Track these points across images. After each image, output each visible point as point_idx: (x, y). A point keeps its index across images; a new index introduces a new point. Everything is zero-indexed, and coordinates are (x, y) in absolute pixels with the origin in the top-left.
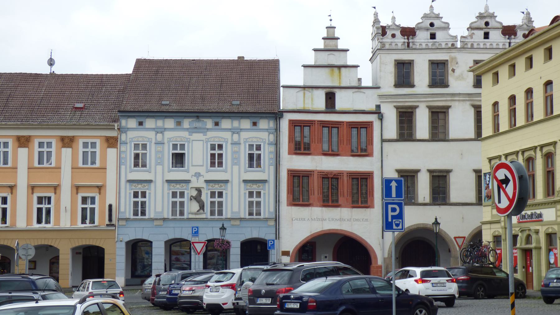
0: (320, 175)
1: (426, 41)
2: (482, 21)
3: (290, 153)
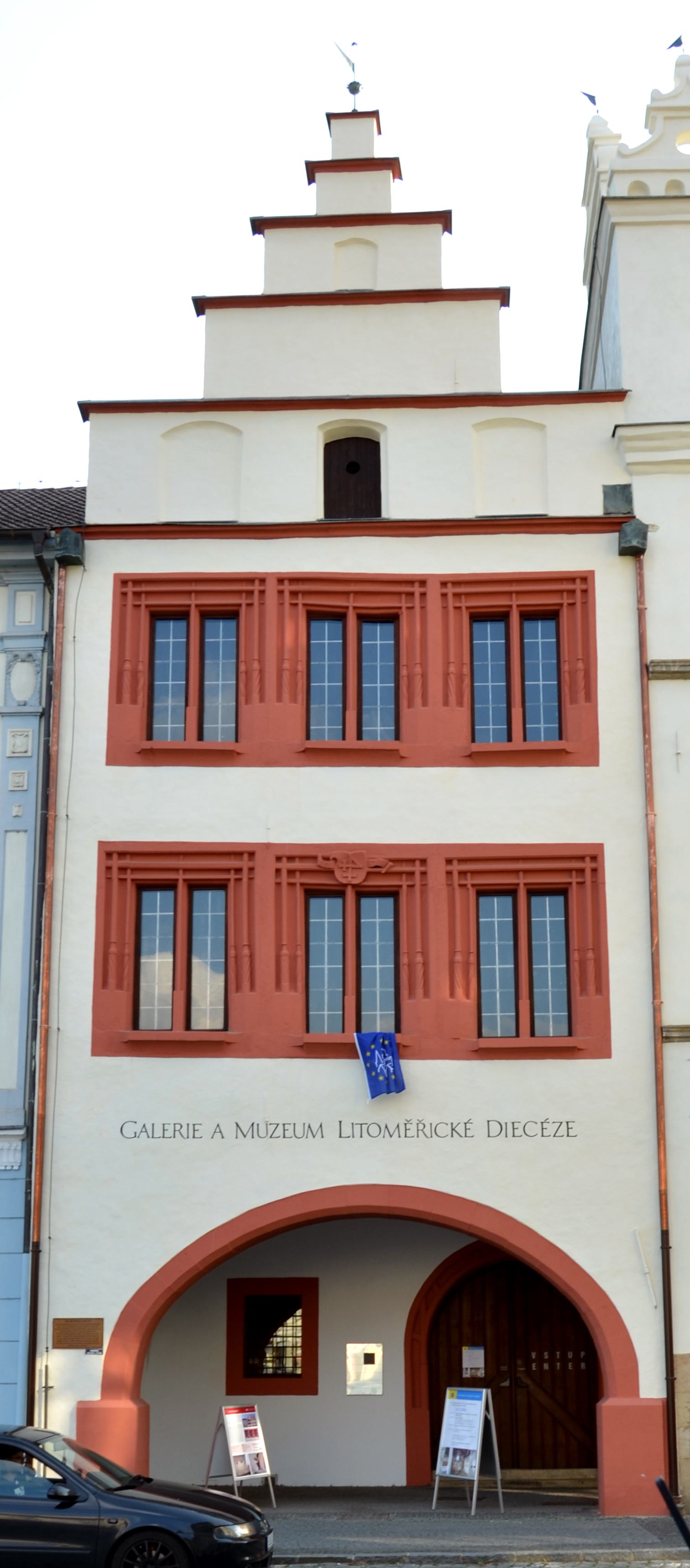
0: (291, 872)
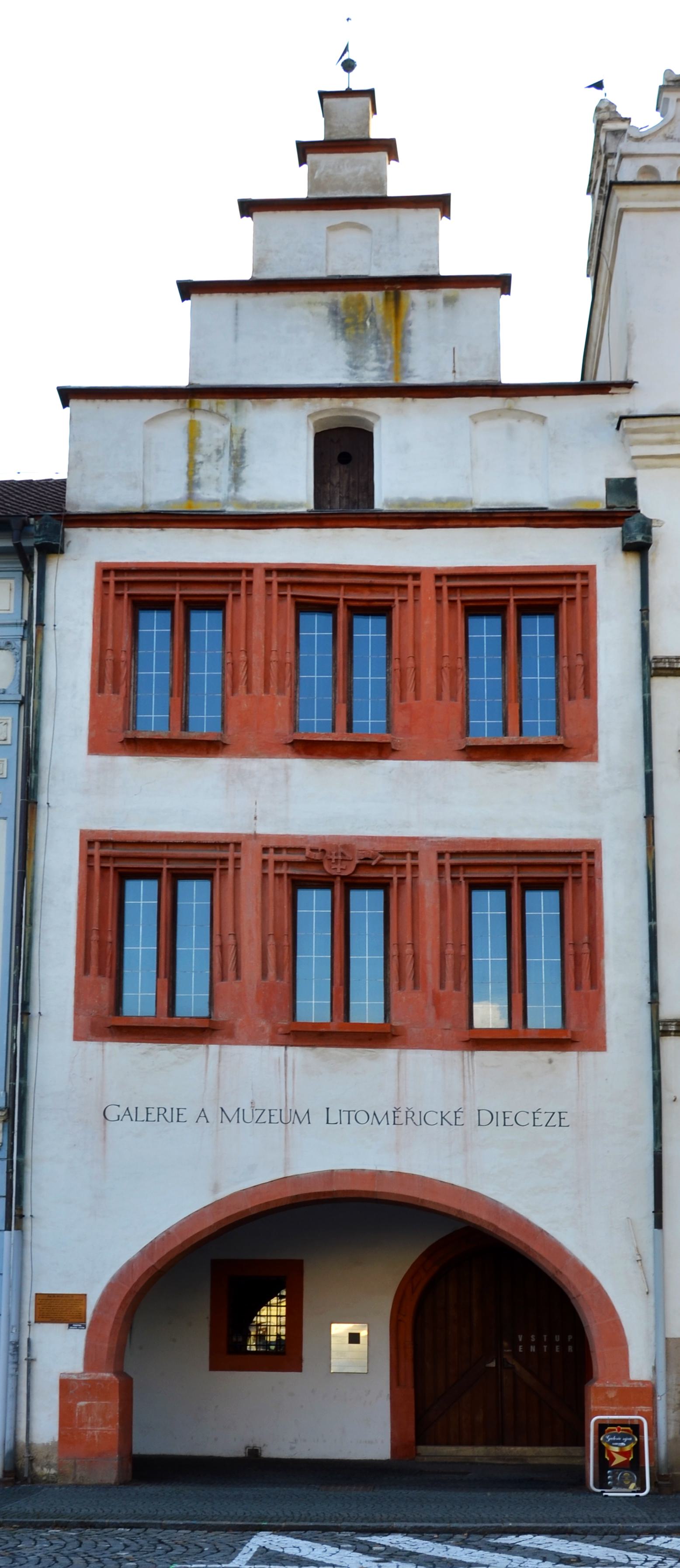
0: (278, 863)
3: (96, 746)
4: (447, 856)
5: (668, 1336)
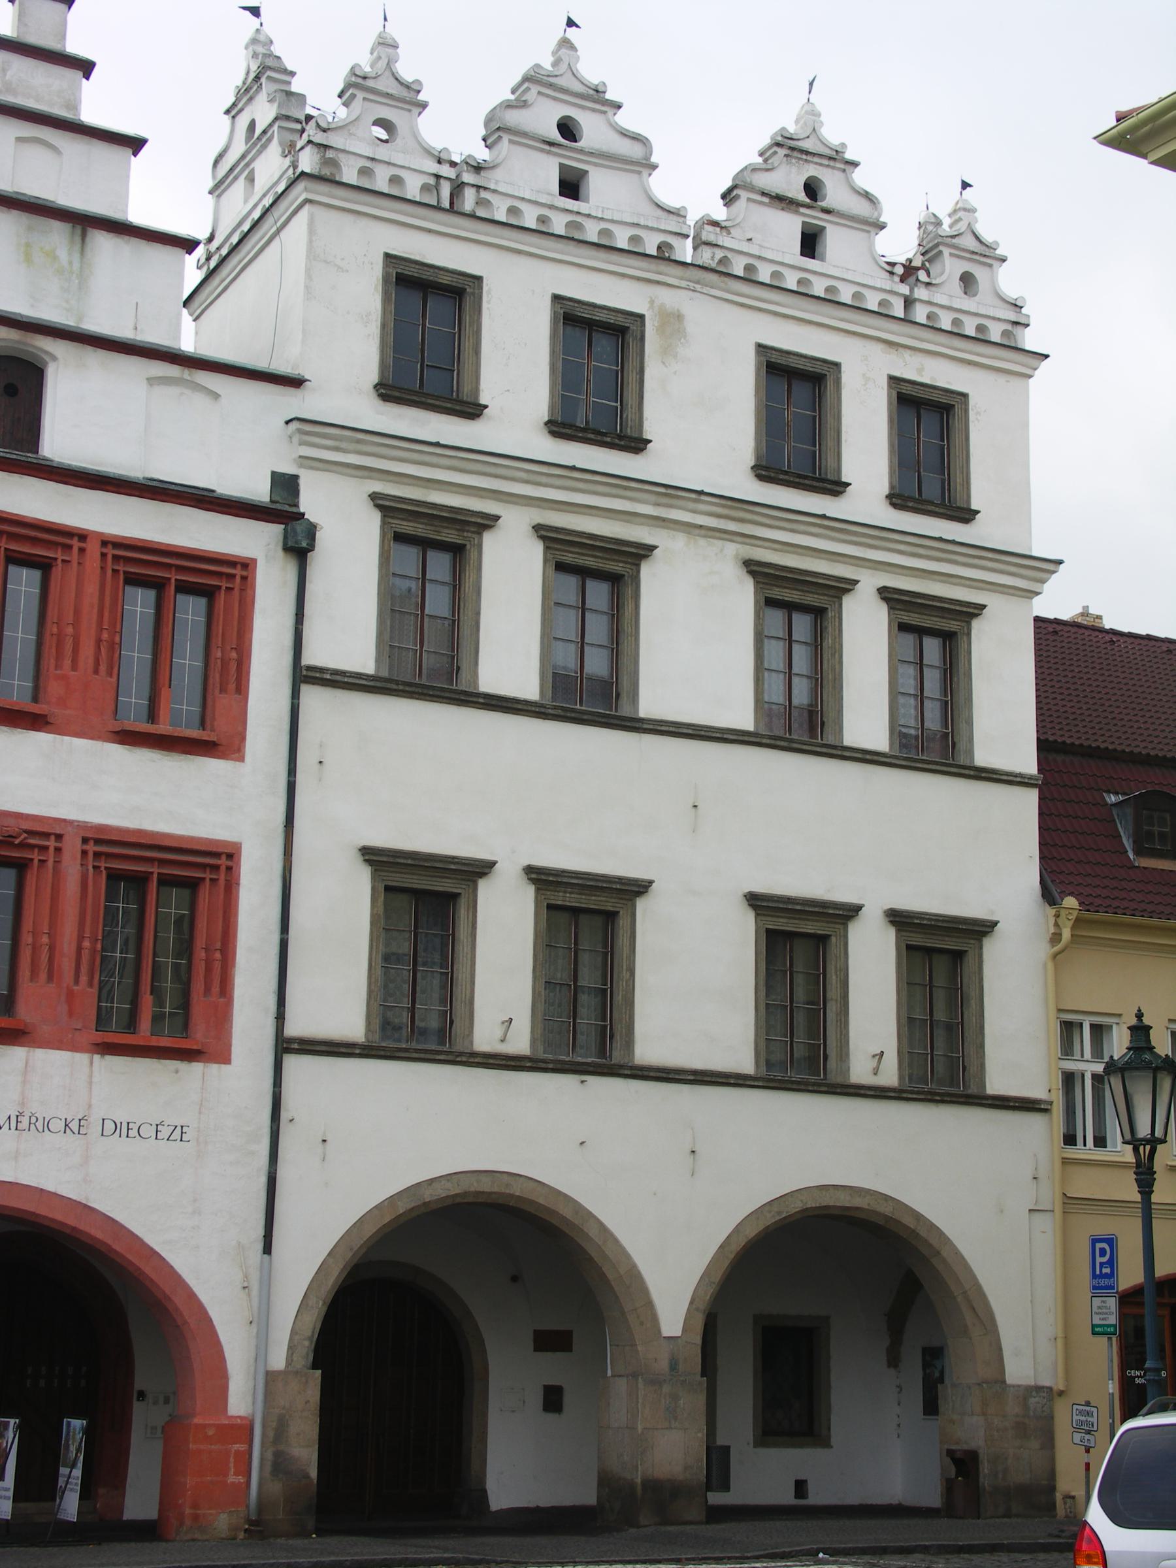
1: (543, 199)
2: (794, 170)
4: (92, 842)
5: (270, 1368)
